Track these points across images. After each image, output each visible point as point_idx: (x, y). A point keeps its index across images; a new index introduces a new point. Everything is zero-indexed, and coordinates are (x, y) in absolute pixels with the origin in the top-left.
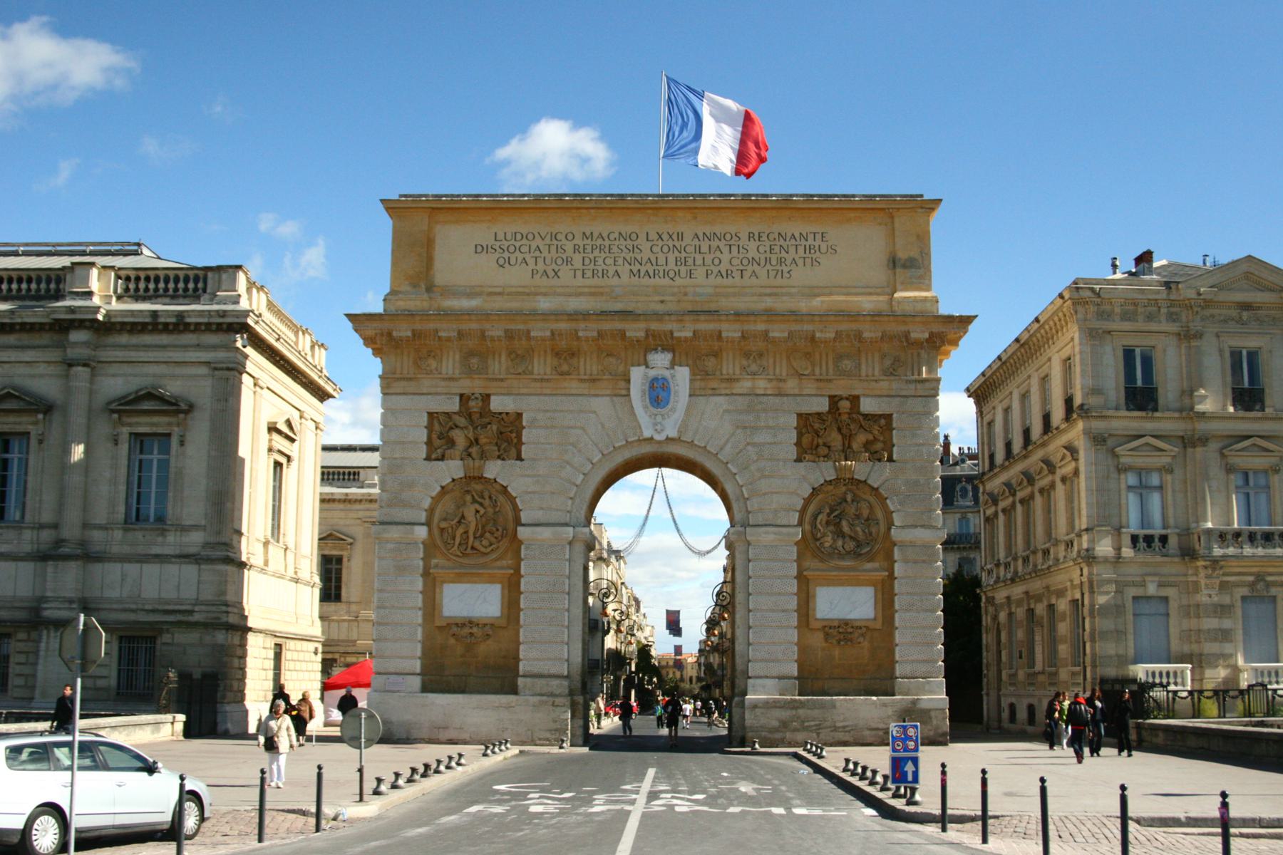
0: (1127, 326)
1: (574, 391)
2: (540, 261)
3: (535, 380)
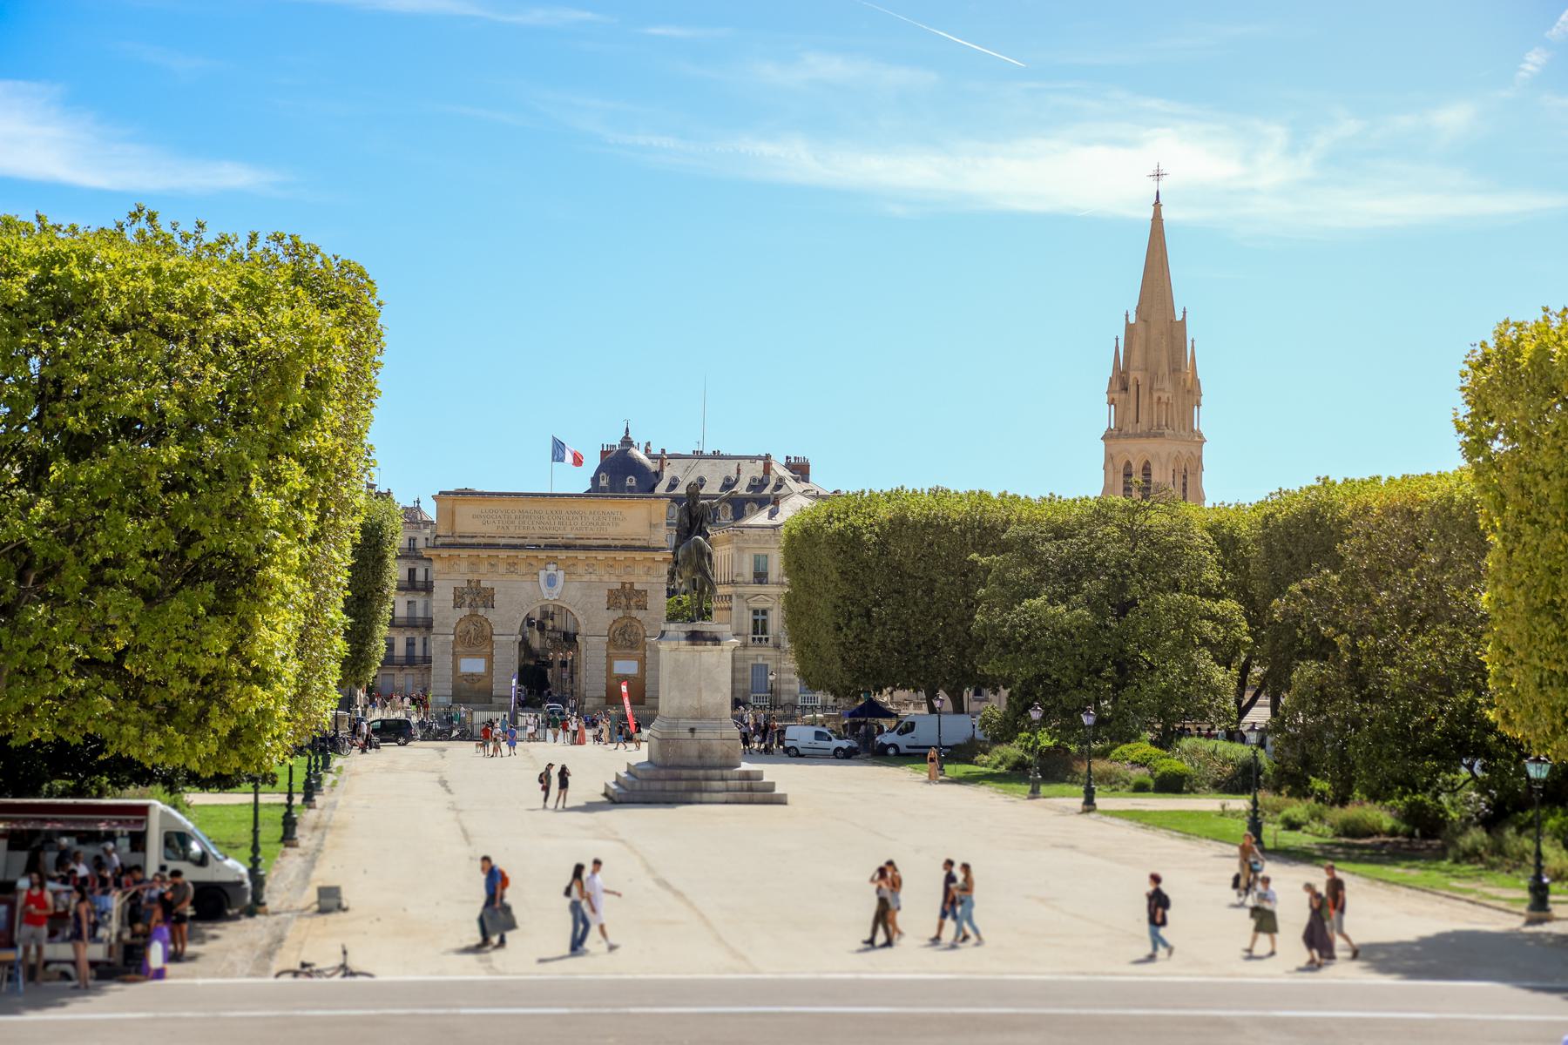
0: (755, 546)
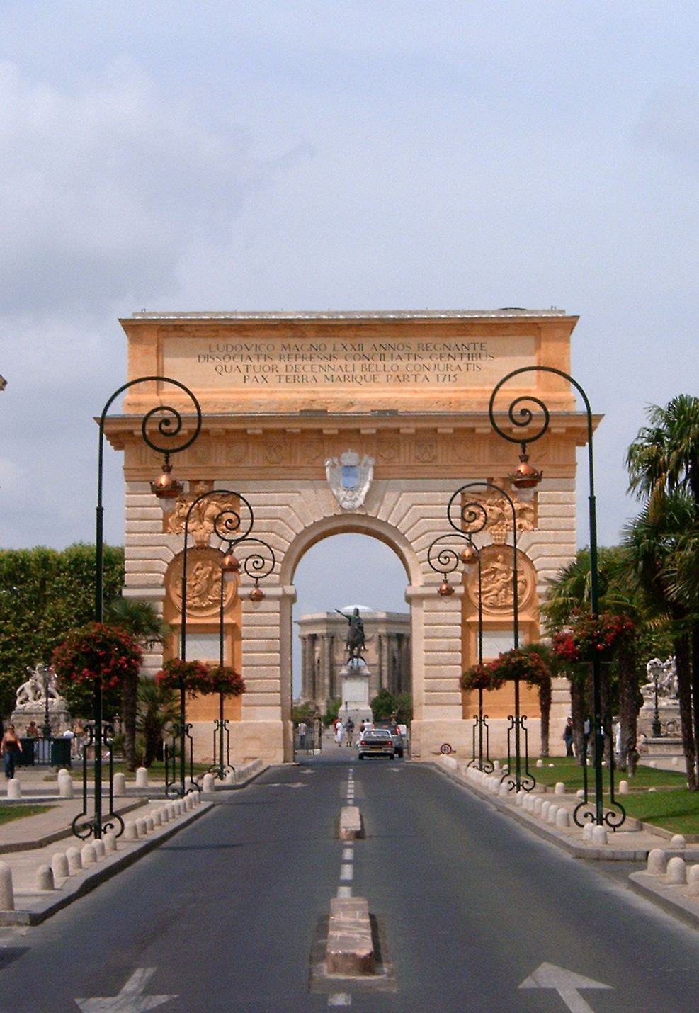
1: (282, 477)
2: (251, 369)
3: (251, 469)
